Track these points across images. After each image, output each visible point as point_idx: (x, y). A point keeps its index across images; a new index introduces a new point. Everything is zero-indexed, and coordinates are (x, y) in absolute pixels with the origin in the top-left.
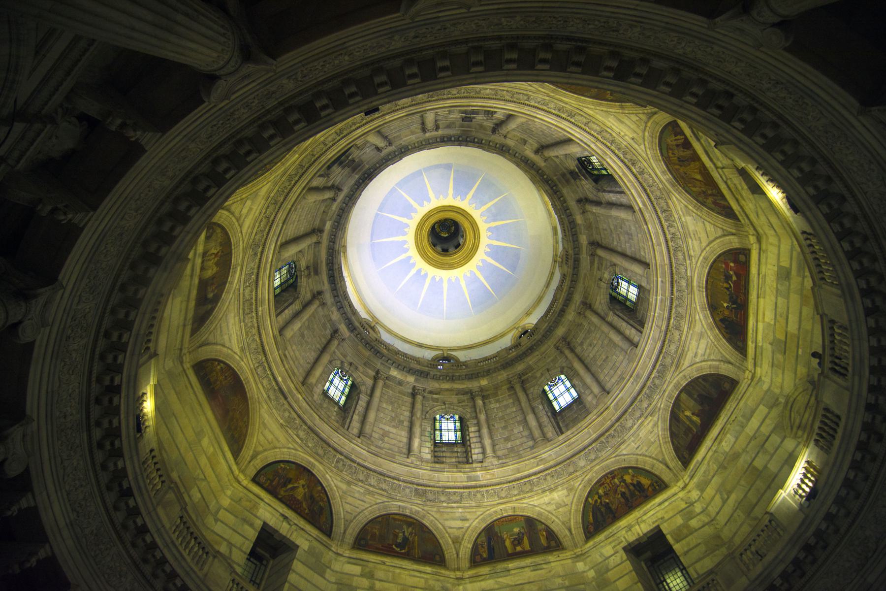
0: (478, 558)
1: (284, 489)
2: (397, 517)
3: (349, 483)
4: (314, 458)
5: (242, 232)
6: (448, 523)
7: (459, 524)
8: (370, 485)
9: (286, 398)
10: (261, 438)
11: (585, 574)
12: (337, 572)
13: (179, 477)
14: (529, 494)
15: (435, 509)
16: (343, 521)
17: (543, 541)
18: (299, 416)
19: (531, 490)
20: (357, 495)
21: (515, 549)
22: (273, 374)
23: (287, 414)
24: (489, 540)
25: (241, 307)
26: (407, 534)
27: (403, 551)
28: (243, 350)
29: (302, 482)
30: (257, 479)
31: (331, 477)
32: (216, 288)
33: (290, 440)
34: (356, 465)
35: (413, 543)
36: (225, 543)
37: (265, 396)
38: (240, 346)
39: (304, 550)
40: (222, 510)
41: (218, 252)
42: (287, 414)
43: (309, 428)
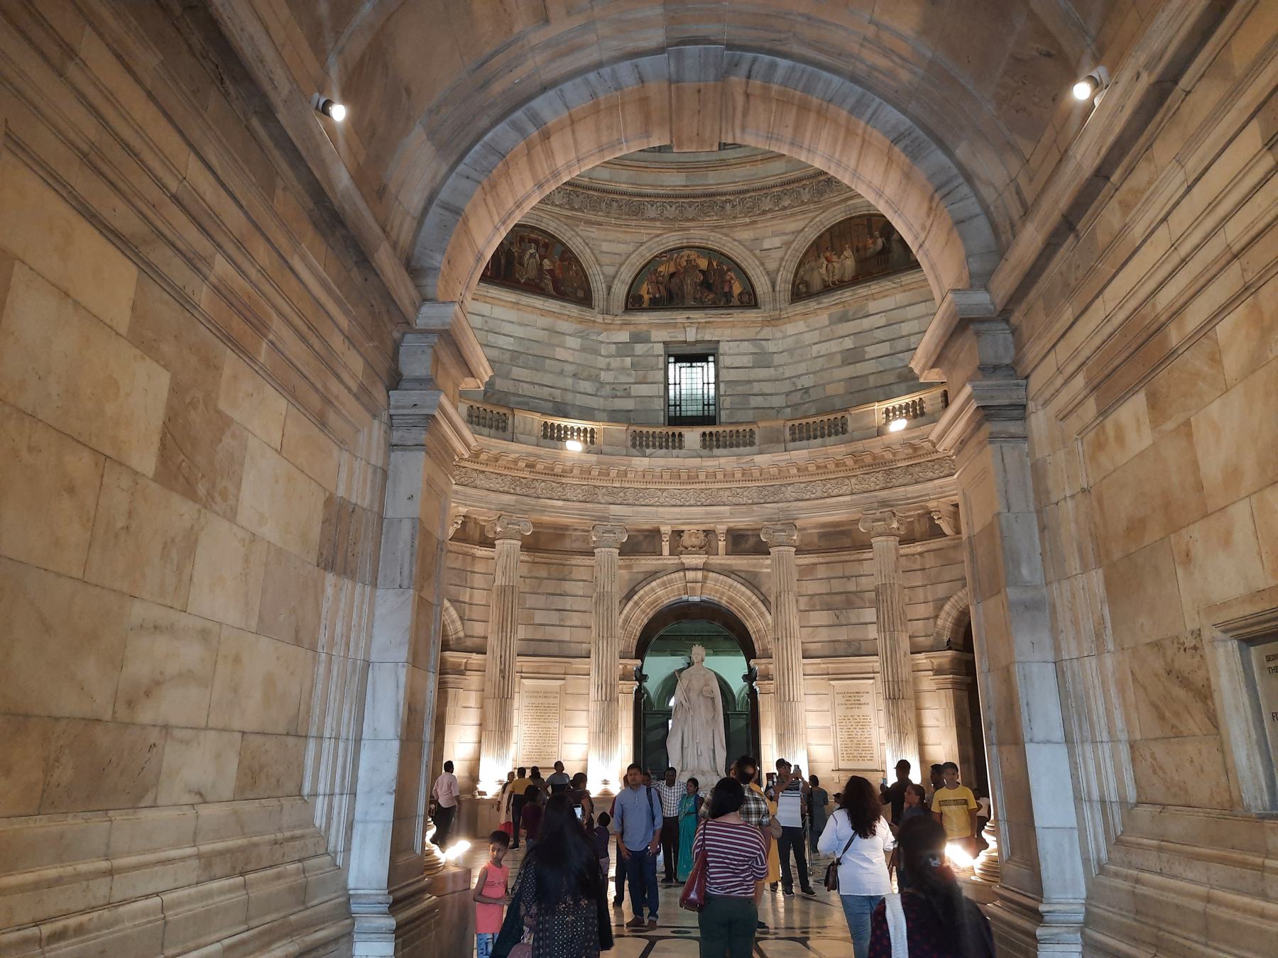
5: (803, 229)
32: (872, 236)
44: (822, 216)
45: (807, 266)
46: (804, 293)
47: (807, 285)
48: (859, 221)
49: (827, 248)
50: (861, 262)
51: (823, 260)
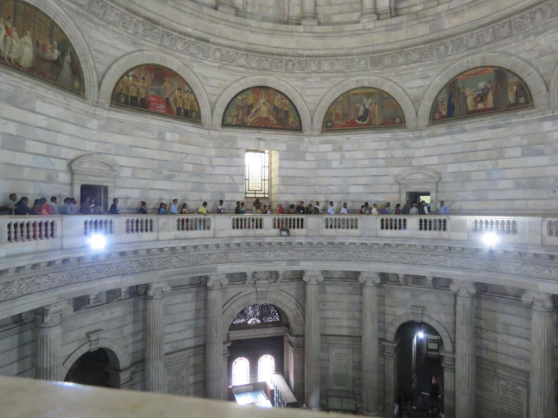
0: (437, 116)
1: (250, 116)
2: (356, 91)
3: (304, 79)
4: (263, 75)
6: (407, 85)
7: (420, 82)
8: (324, 72)
9: (207, 41)
10: (210, 90)
11: (550, 134)
12: (314, 152)
13: (169, 171)
14: (506, 41)
15: (393, 74)
16: (308, 113)
17: (511, 98)
18: (230, 47)
19: (510, 35)
20: (315, 85)
21: (476, 106)
22: (180, 33)
23: (218, 54)
24: (450, 97)
25: (92, 16)
26: (367, 106)
27: (365, 123)
28: (134, 43)
29: (262, 101)
30: (225, 123)
31: (285, 82)
32: (51, 43)
33: (235, 73)
34: (305, 59)
35: (374, 113)
36: (227, 177)
37: (188, 57)
38: (129, 43)
39: (285, 151)
40: (214, 159)
41: (7, 28)
42: (218, 54)
43: (246, 50)
50: (39, 58)
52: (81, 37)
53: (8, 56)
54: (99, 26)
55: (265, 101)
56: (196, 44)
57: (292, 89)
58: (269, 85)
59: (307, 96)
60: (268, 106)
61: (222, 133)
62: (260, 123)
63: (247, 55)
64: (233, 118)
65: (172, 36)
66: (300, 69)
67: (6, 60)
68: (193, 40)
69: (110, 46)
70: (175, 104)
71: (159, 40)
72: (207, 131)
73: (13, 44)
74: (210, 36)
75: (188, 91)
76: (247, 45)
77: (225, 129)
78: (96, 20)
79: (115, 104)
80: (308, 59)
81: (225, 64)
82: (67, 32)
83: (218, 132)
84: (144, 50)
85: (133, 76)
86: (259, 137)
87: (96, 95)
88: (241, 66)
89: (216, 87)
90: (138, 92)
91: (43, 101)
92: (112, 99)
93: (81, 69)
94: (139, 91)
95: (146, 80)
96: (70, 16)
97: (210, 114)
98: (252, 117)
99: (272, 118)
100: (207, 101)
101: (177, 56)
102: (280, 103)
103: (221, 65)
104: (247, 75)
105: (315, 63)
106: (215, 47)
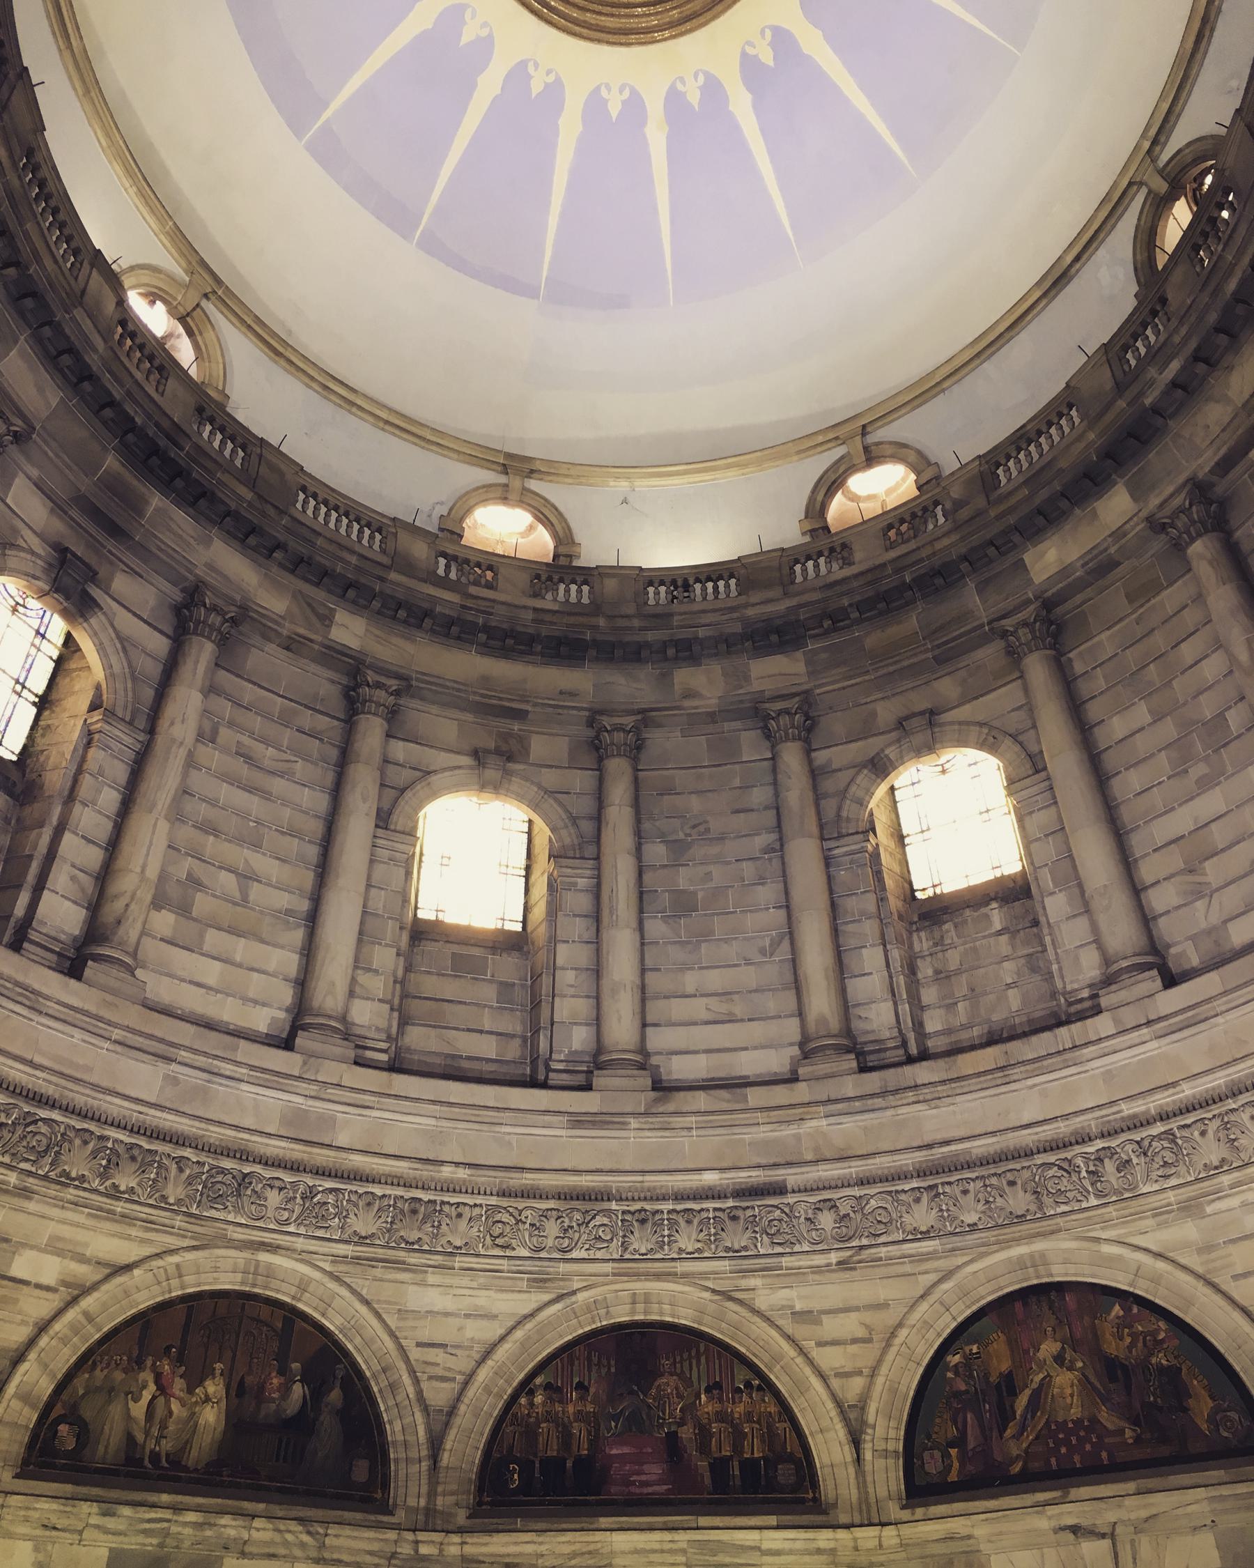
3: (1190, 1208)
4: (1018, 1241)
9: (779, 1190)
10: (830, 1359)
18: (862, 1182)
23: (827, 1220)
25: (401, 1255)
28: (540, 1282)
29: (1048, 1348)
30: (919, 1481)
32: (282, 1371)
33: (908, 1268)
34: (1159, 1128)
37: (724, 1265)
42: (827, 1220)
43: (921, 1173)
44: (190, 1256)
45: (99, 1374)
46: (67, 1455)
47: (84, 1432)
48: (265, 1311)
49: (168, 1348)
51: (147, 1376)
52: (374, 1322)
53: (152, 1451)
54: (426, 1272)
55: (1059, 1345)
56: (740, 1213)
57: (1161, 1265)
58: (1060, 1274)
59: (1236, 1277)
60: (1080, 1364)
61: (906, 1530)
62: (1063, 1450)
63: (931, 1187)
64: (945, 1455)
65: (658, 1217)
66: (1154, 1176)
67: (146, 1462)
68: (730, 1203)
69: (467, 1316)
70: (704, 1448)
71: (617, 1242)
72: (842, 1534)
73: (171, 1413)
74: (782, 1171)
75: (748, 1385)
76: (920, 1156)
77: (920, 1512)
78: (412, 1261)
79: (492, 1504)
80: (1173, 1124)
81: (862, 1248)
82: (332, 1323)
83: (889, 1531)
84: (574, 1293)
85: (548, 1387)
86: (1070, 1521)
87: (424, 1489)
88: (926, 1235)
89: (855, 1341)
90: (566, 1438)
91: (243, 1555)
92: (480, 1490)
93: (378, 1415)
94: (571, 1435)
95: (592, 1390)
96: (337, 1279)
97: (848, 1453)
98: (1023, 1428)
99: (1107, 1419)
100: (830, 1405)
101: (685, 1275)
102: (1128, 1340)
103: (849, 1253)
104: (960, 1260)
105: (1210, 1133)
106: (812, 1199)
